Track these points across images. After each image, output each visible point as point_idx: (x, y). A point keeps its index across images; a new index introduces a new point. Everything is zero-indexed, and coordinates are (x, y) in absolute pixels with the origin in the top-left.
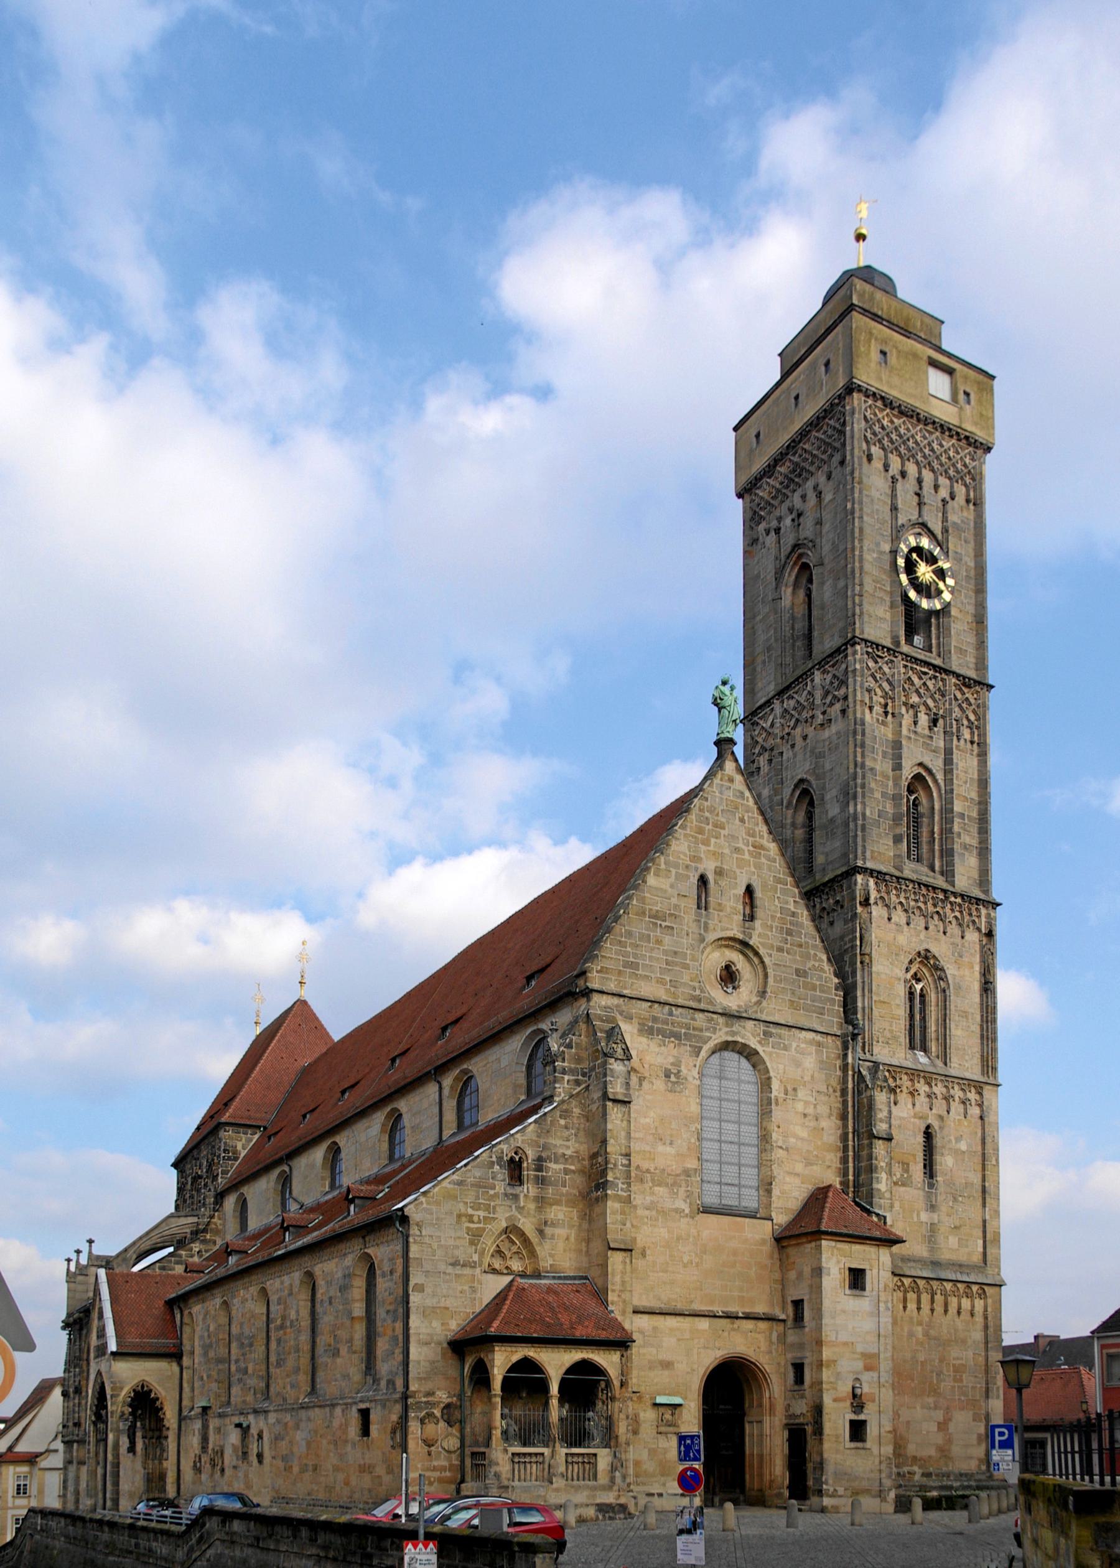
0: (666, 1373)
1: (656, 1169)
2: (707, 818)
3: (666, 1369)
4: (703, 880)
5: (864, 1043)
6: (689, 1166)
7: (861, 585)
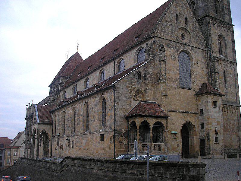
0: (174, 126)
3: (175, 124)
4: (177, 15)
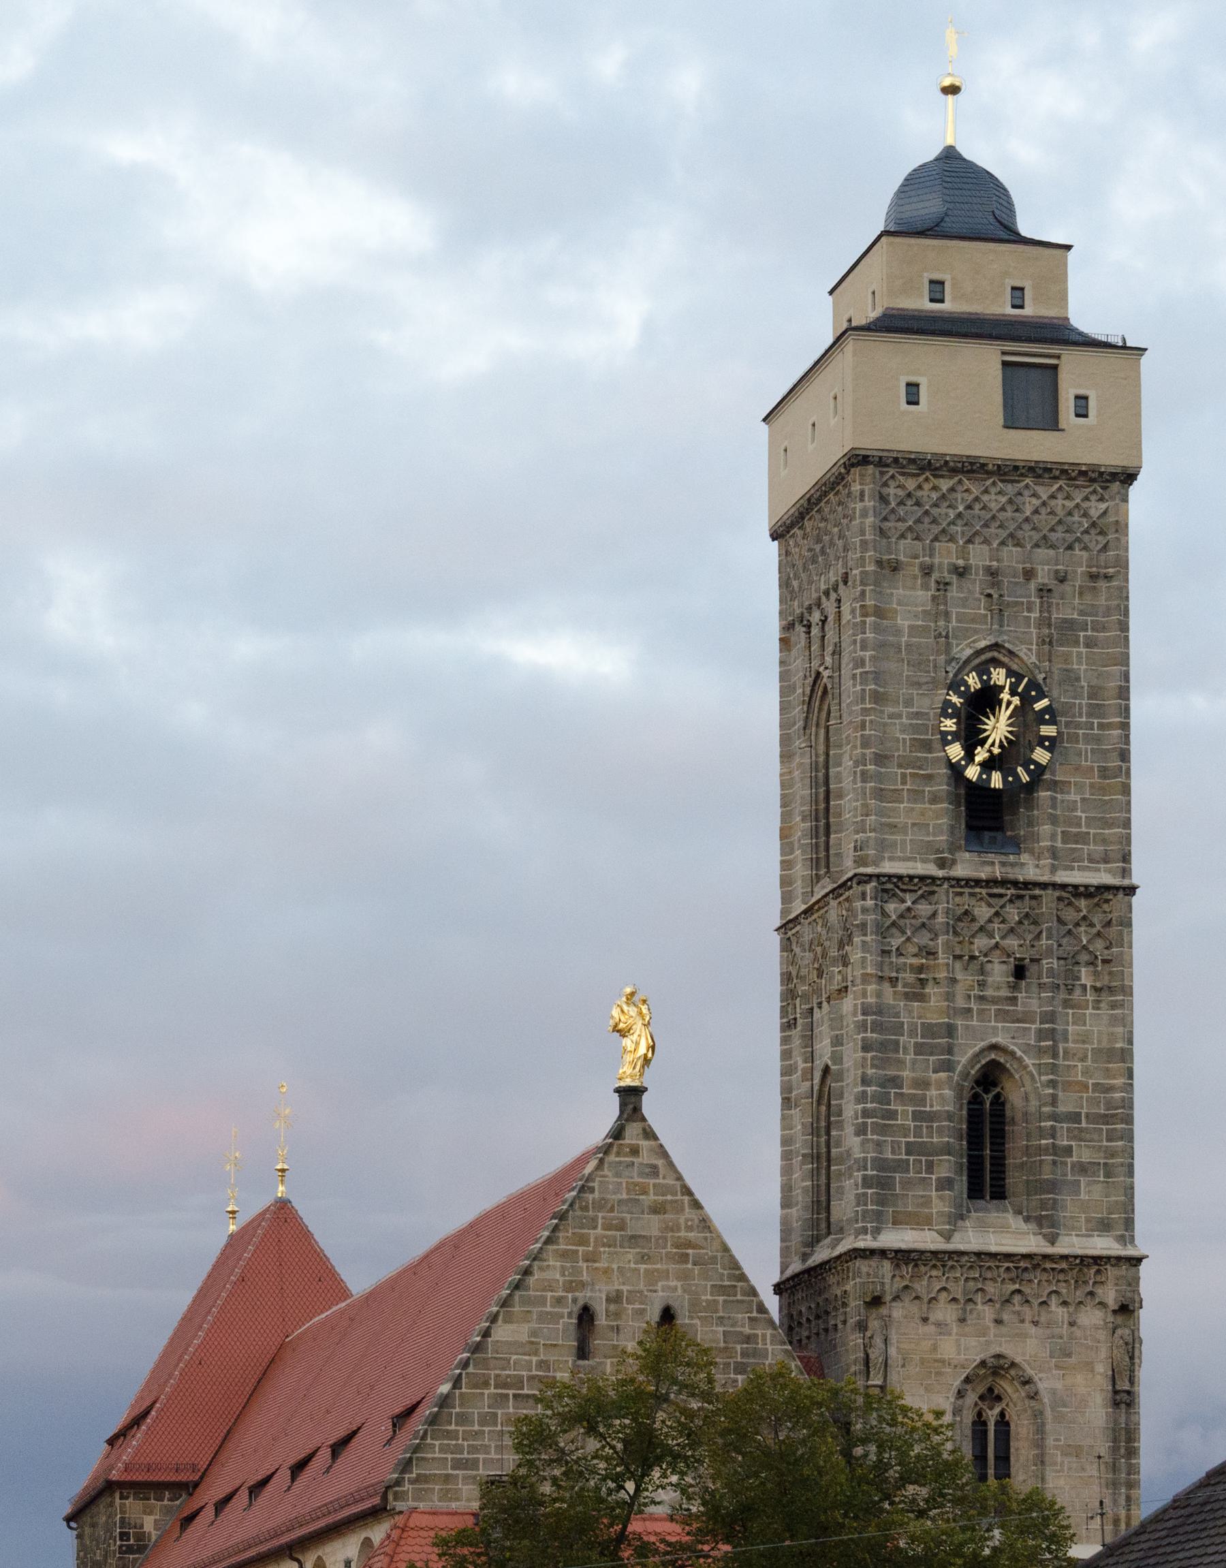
4: (586, 1316)
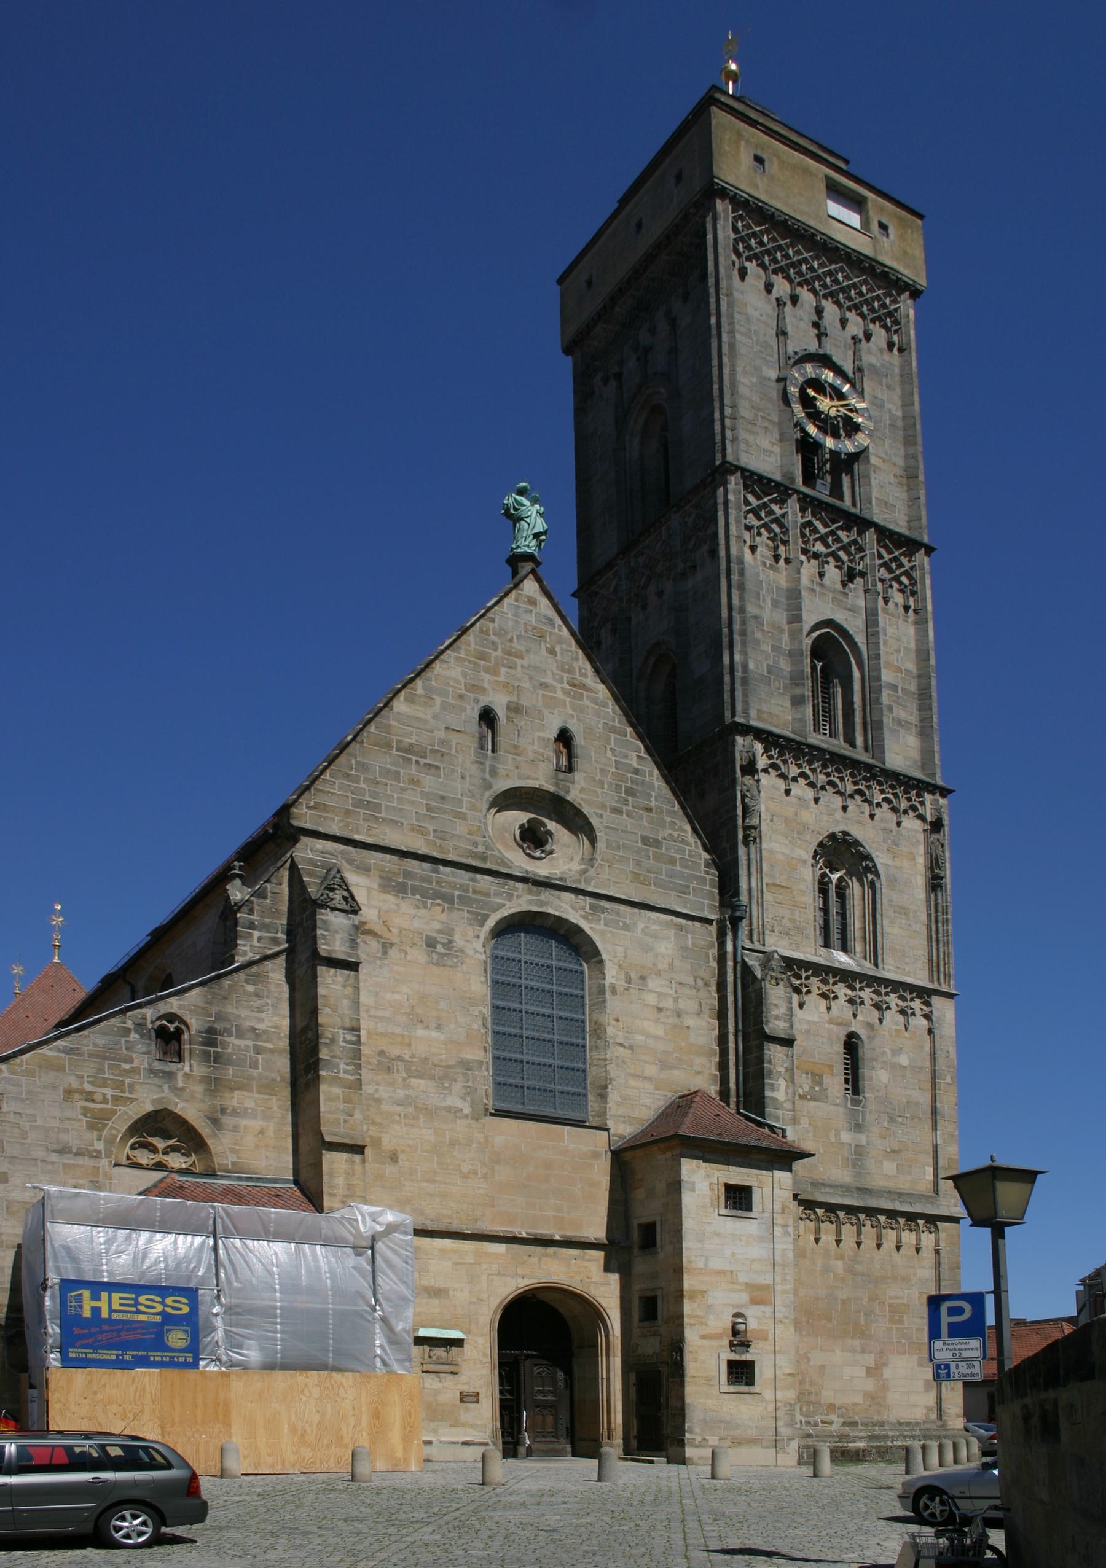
1: (413, 1056)
2: (493, 643)
5: (751, 931)
6: (470, 1057)
7: (734, 406)
